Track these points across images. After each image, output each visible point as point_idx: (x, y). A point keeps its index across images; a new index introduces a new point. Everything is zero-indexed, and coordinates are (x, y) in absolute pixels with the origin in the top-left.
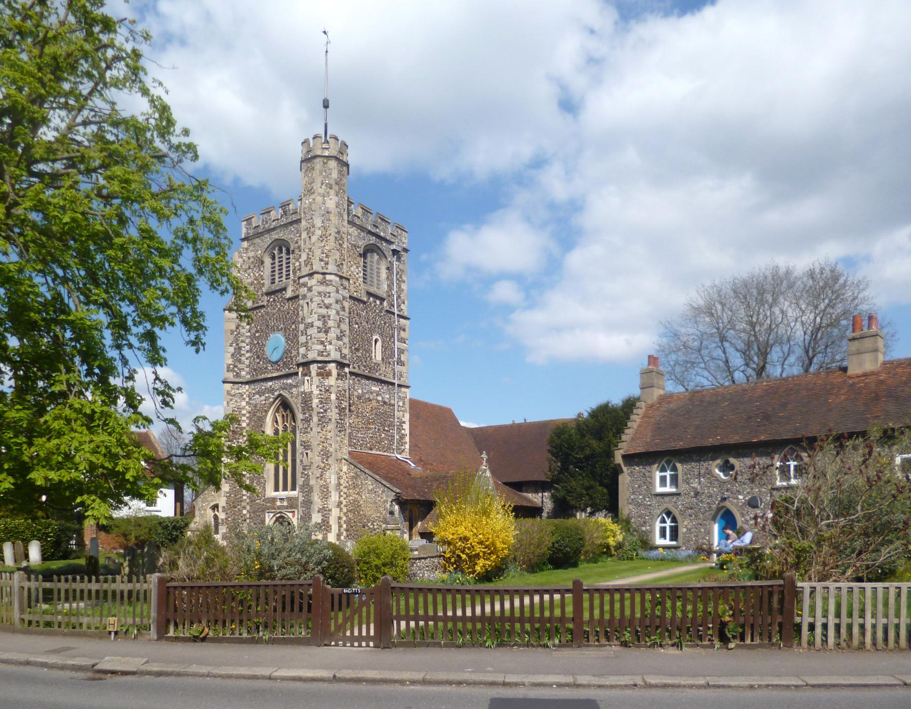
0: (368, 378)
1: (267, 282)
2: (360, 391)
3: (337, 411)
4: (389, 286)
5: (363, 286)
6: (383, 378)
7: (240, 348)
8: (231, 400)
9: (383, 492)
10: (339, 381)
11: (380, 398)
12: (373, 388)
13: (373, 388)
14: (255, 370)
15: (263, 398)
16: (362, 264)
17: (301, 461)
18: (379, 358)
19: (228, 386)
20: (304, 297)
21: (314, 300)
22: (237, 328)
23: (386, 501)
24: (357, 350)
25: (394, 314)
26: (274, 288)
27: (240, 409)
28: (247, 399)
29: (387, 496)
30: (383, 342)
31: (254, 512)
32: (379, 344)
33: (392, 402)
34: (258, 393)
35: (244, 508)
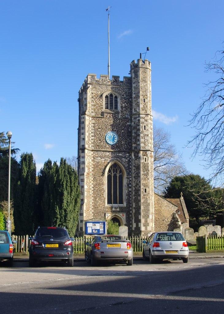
28: (93, 159)
31: (97, 213)
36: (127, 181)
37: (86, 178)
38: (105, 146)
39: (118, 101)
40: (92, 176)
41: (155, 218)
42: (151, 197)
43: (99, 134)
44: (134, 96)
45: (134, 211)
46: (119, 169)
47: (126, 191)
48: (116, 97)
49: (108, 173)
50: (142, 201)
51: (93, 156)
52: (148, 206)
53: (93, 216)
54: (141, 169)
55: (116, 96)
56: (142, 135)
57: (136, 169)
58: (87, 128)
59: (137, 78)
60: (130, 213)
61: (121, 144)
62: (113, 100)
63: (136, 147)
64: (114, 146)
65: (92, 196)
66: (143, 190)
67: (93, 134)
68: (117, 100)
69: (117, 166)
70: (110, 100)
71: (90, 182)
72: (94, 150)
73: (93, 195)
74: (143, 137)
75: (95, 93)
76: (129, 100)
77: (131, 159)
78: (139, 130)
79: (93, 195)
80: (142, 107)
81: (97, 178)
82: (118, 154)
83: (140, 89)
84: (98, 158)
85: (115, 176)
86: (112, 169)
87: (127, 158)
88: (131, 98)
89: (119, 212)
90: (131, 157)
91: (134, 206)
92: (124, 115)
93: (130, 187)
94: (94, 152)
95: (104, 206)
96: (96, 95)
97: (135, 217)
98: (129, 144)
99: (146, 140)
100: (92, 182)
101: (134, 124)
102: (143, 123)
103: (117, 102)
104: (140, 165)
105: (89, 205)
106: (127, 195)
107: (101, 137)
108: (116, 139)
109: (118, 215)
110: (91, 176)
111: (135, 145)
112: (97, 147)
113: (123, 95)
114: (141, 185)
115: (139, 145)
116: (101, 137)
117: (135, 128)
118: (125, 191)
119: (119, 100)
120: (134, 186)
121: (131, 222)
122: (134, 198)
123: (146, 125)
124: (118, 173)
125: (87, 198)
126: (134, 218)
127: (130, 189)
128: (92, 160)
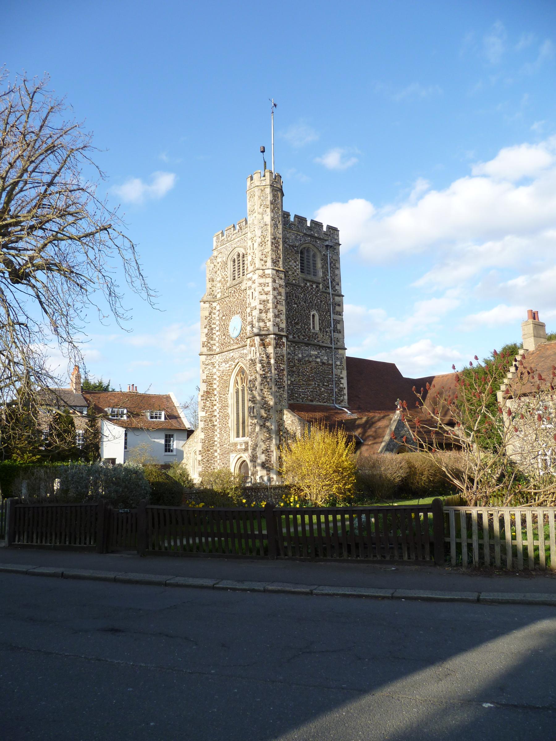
0: (307, 345)
1: (229, 279)
2: (300, 356)
3: (276, 372)
4: (323, 273)
5: (301, 275)
6: (321, 344)
7: (212, 329)
8: (206, 368)
10: (278, 349)
11: (318, 360)
12: (312, 352)
13: (312, 352)
14: (222, 344)
15: (228, 365)
16: (299, 258)
18: (317, 328)
19: (203, 357)
20: (250, 288)
21: (256, 289)
22: (210, 314)
24: (297, 324)
25: (329, 294)
26: (235, 282)
27: (212, 374)
28: (217, 367)
30: (320, 316)
32: (317, 318)
33: (330, 362)
35: (216, 451)
43: (224, 324)
71: (215, 405)
73: (218, 426)
105: (209, 442)
110: (215, 395)
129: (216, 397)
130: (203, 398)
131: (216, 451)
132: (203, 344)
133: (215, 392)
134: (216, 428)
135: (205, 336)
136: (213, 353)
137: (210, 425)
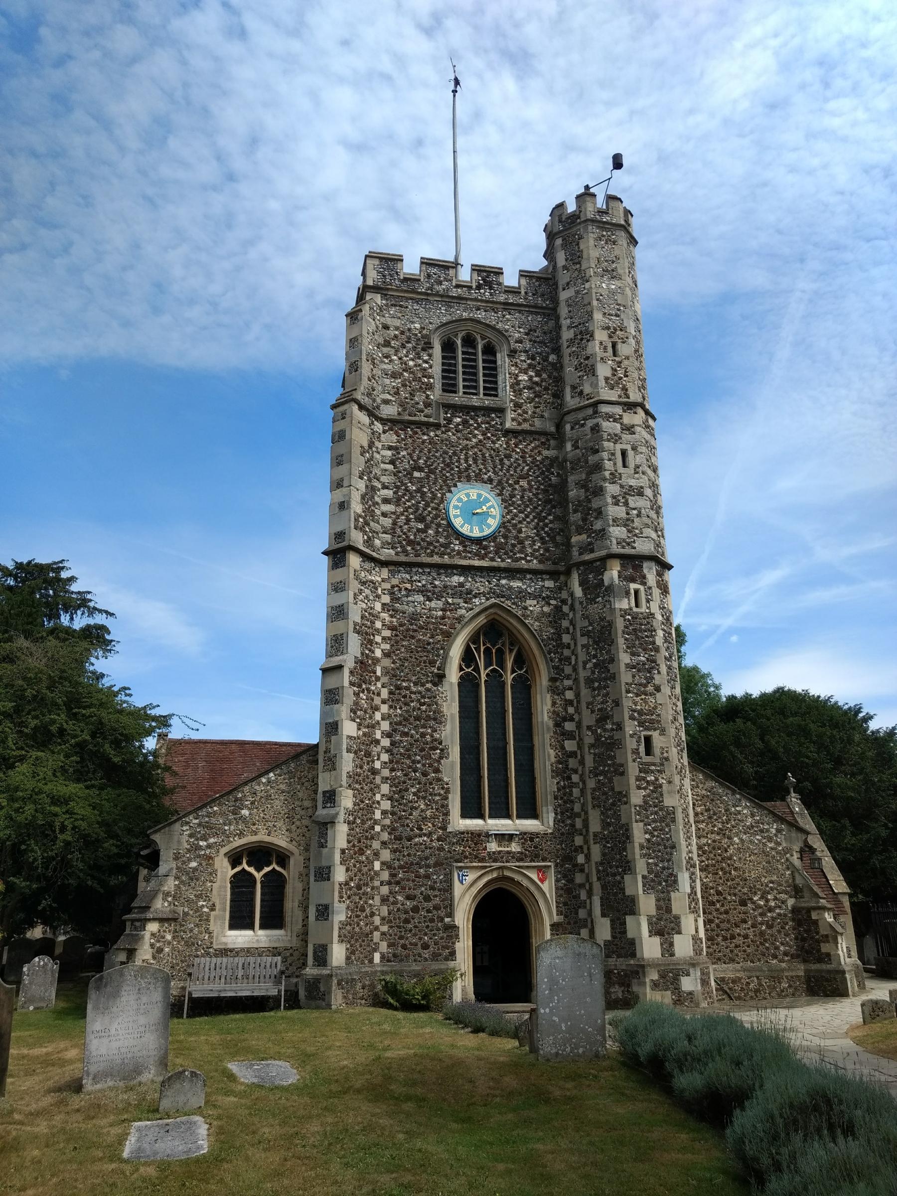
9: (779, 831)
17: (636, 752)
23: (788, 850)
28: (386, 599)
29: (788, 839)
34: (422, 591)
36: (554, 704)
37: (352, 684)
38: (446, 546)
39: (499, 362)
40: (385, 679)
41: (705, 888)
42: (677, 779)
43: (418, 490)
44: (567, 335)
45: (596, 852)
46: (511, 651)
47: (552, 753)
48: (490, 350)
49: (461, 669)
50: (637, 797)
51: (387, 586)
52: (668, 825)
53: (389, 883)
54: (621, 641)
55: (489, 343)
56: (612, 489)
57: (595, 642)
58: (362, 460)
59: (579, 263)
60: (576, 865)
61: (516, 538)
62: (475, 360)
63: (590, 544)
64: (485, 548)
65: (385, 780)
66: (638, 742)
67: (389, 493)
68: (495, 362)
69: (500, 635)
70: (463, 359)
71: (377, 709)
72: (396, 558)
73: (386, 773)
74: (620, 498)
75: (397, 328)
76: (545, 359)
77: (564, 602)
78: (598, 467)
79: (386, 773)
80: (609, 374)
81: (407, 688)
82: (503, 582)
83: (595, 303)
84: (410, 599)
85: (495, 679)
86: (478, 649)
87: (548, 597)
88: (557, 350)
89: (521, 857)
90: (564, 595)
91: (595, 826)
92: (525, 420)
93: (570, 736)
94: (392, 568)
95: (444, 828)
96: (402, 333)
97: (604, 887)
98: (553, 539)
99: (635, 512)
100: (384, 708)
101: (575, 446)
102: (616, 438)
103: (495, 369)
104: (611, 624)
105: (363, 822)
106: (556, 773)
107: (427, 505)
108: (494, 517)
109: (517, 877)
111: (584, 536)
112: (409, 548)
113: (520, 342)
114: (626, 716)
115: (602, 534)
116: (427, 505)
117: (576, 463)
118: (546, 756)
119: (502, 359)
120: (589, 728)
121: (582, 914)
122: (591, 784)
123: (629, 447)
124: (509, 665)
125: (357, 786)
126: (597, 887)
127: (570, 745)
128: (383, 604)
129: (379, 685)
130: (353, 679)
131: (376, 854)
132: (356, 520)
133: (379, 673)
134: (378, 780)
135: (359, 498)
136: (374, 554)
137: (366, 767)
